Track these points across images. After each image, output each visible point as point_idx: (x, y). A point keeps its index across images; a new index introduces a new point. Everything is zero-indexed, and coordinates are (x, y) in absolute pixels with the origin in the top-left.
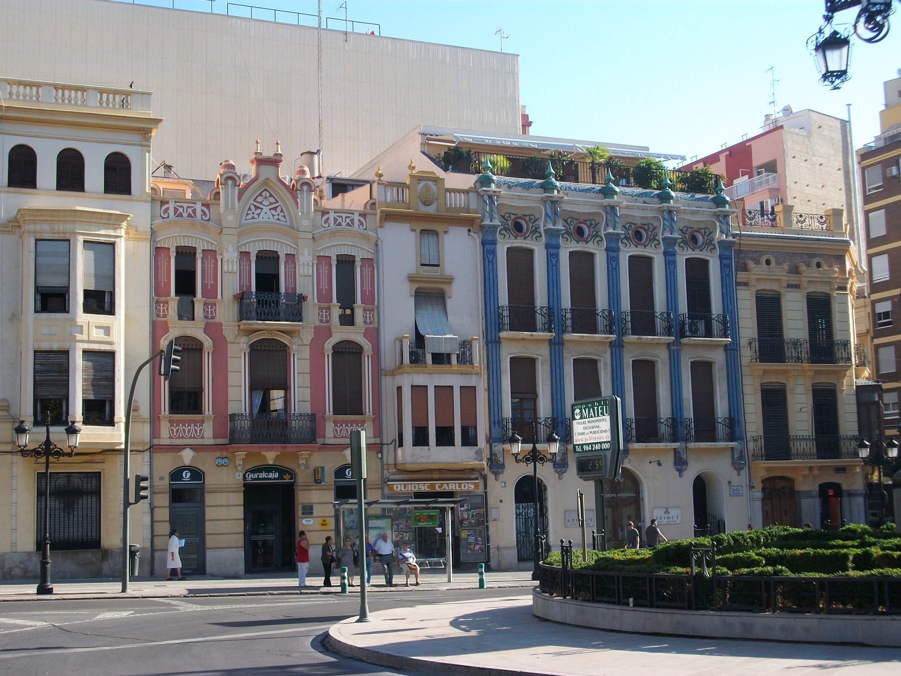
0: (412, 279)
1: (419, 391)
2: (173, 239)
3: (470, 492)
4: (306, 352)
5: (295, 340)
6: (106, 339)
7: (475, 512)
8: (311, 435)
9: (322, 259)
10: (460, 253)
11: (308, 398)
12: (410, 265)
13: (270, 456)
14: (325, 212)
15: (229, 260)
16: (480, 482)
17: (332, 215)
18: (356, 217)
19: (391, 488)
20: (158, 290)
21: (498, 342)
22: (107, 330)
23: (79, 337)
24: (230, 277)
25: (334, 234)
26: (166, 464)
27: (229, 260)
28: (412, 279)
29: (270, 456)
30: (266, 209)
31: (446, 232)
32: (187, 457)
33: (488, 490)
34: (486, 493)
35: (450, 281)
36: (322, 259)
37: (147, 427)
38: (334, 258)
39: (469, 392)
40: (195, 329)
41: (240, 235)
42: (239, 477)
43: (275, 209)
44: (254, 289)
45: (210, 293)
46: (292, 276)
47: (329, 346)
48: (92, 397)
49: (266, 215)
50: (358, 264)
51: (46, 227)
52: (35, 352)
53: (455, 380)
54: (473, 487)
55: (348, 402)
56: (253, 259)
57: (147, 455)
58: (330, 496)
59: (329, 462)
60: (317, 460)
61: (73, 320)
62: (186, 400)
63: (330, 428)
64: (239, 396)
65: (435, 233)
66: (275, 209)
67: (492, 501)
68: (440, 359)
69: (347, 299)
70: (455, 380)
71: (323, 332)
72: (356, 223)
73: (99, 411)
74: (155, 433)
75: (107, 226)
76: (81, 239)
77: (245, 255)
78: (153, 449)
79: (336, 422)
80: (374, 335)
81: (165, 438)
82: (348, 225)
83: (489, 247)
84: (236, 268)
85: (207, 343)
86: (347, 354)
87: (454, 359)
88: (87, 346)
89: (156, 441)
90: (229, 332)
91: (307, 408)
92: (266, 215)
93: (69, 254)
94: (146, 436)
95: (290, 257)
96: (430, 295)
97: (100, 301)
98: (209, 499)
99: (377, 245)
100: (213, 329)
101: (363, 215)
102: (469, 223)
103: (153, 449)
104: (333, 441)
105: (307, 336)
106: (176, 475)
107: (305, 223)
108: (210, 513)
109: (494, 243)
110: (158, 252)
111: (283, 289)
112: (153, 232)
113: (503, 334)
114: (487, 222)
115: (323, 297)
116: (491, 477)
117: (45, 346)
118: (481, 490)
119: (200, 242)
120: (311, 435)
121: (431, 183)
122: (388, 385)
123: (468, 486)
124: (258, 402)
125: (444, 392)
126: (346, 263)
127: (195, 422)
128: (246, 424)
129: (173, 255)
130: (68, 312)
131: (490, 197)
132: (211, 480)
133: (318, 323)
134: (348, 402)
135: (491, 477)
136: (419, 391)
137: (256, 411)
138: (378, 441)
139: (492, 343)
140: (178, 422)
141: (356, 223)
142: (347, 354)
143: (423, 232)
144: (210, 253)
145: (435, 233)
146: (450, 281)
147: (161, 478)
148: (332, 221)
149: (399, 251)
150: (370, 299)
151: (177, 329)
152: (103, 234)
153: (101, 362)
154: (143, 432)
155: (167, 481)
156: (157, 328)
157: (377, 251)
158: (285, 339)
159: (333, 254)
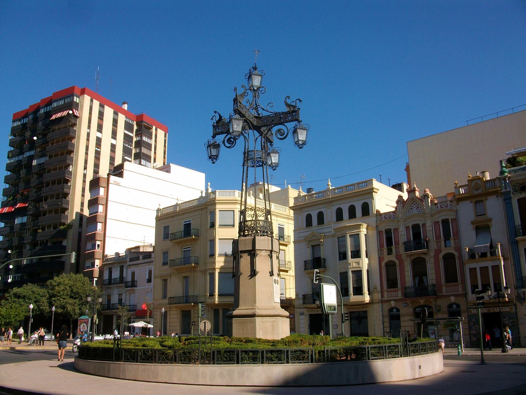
0: (473, 223)
1: (473, 271)
2: (383, 228)
3: (508, 312)
4: (432, 260)
5: (427, 256)
6: (358, 266)
7: (511, 321)
8: (435, 293)
9: (436, 223)
10: (494, 207)
11: (434, 278)
12: (472, 217)
13: (422, 302)
14: (436, 204)
15: (402, 231)
16: (514, 307)
17: (439, 205)
18: (449, 203)
19: (470, 311)
20: (381, 246)
21: (517, 242)
22: (358, 263)
23: (349, 267)
24: (403, 236)
25: (439, 212)
26: (387, 307)
27: (402, 231)
28: (473, 223)
29: (422, 302)
30: (415, 209)
31: (486, 200)
32: (393, 303)
33: (518, 310)
34: (516, 312)
35: (490, 220)
36: (436, 223)
37: (380, 294)
38: (440, 221)
39: (496, 269)
40: (393, 258)
41: (405, 221)
42: (411, 310)
43: (418, 208)
44: (412, 239)
45: (397, 244)
46: (425, 231)
47: (441, 256)
48: (356, 286)
49: (415, 211)
50: (450, 221)
51: (340, 233)
52: (340, 273)
53: (489, 264)
54: (509, 309)
55: (451, 276)
56: (410, 228)
57: (380, 304)
58: (446, 316)
59: (443, 303)
60: (440, 302)
61: (348, 262)
62: (392, 283)
63: (444, 289)
64: (409, 280)
65: (482, 201)
66: (418, 208)
67: (520, 315)
68: (484, 255)
69: (447, 237)
70: (489, 264)
71: (438, 251)
72: (449, 205)
73: (358, 291)
74: (382, 296)
75: (356, 229)
76: (348, 235)
77: (408, 227)
78: (382, 302)
79: (446, 286)
80: (459, 249)
81: (386, 298)
82: (446, 207)
83: (508, 201)
84: (404, 233)
85: (397, 262)
86: (449, 259)
87: (489, 254)
88: (352, 269)
89: (383, 299)
90: (404, 257)
91: (434, 282)
92: (415, 211)
93: (345, 241)
94: (380, 298)
95: (424, 225)
96: (482, 228)
97: (356, 254)
98: (402, 319)
99: (457, 212)
100: (398, 257)
101: (451, 201)
102: (496, 193)
103: (382, 302)
104: (445, 294)
105: (432, 254)
106: (391, 310)
107: (427, 210)
108: (402, 324)
109: (510, 199)
110: (379, 233)
111: (422, 238)
112: (377, 227)
113: (518, 238)
114: (504, 191)
115: (438, 237)
116: (518, 304)
117: (342, 271)
118: (514, 310)
119: (392, 226)
120: (435, 293)
121: (478, 181)
122: (467, 267)
123: (506, 309)
124: (417, 281)
125: (484, 270)
126: (445, 222)
127: (395, 291)
128: (412, 290)
129: (384, 232)
130: (360, 257)
131: (504, 179)
132: (402, 311)
133: (436, 248)
134: (451, 276)
135: (518, 304)
136: (473, 271)
137: (416, 285)
138: (464, 292)
139: (514, 244)
140: (391, 291)
141: (449, 205)
142: (449, 259)
143: (476, 202)
144: (396, 230)
145: (482, 201)
146: (490, 220)
147: (386, 312)
148: (439, 207)
149: (467, 213)
150: (457, 234)
151: (387, 258)
152: (354, 232)
153: (358, 274)
154: (377, 296)
155: (387, 313)
156: (380, 260)
157: (457, 215)
158: (423, 256)
159: (440, 220)
